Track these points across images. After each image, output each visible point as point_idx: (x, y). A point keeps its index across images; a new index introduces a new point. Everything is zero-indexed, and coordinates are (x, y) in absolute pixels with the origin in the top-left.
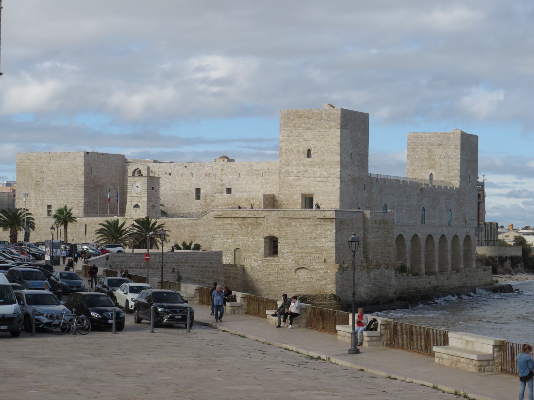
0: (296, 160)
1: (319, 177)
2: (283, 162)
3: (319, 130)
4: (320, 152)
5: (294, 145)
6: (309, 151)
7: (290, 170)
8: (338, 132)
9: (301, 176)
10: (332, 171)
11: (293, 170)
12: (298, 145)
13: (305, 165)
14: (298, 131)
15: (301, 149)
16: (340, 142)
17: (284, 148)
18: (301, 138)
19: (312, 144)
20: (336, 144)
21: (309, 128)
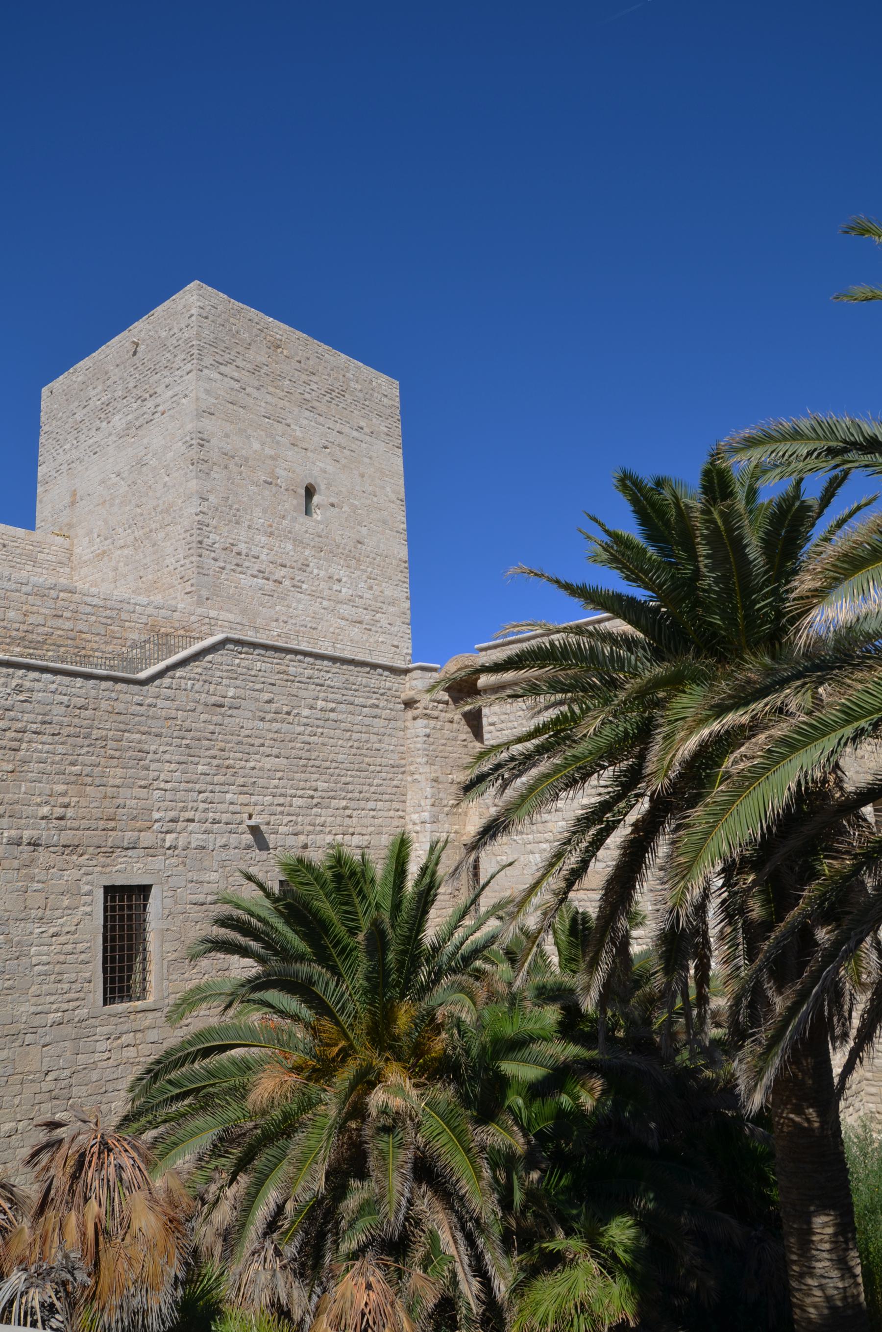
0: (265, 511)
1: (350, 601)
2: (212, 498)
3: (338, 427)
4: (346, 508)
5: (256, 446)
6: (310, 492)
7: (242, 547)
8: (398, 463)
9: (287, 583)
10: (388, 593)
11: (255, 550)
12: (268, 451)
13: (298, 542)
14: (269, 398)
15: (280, 472)
16: (402, 495)
17: (214, 441)
18: (280, 428)
19: (319, 468)
20: (393, 497)
21: (305, 404)
